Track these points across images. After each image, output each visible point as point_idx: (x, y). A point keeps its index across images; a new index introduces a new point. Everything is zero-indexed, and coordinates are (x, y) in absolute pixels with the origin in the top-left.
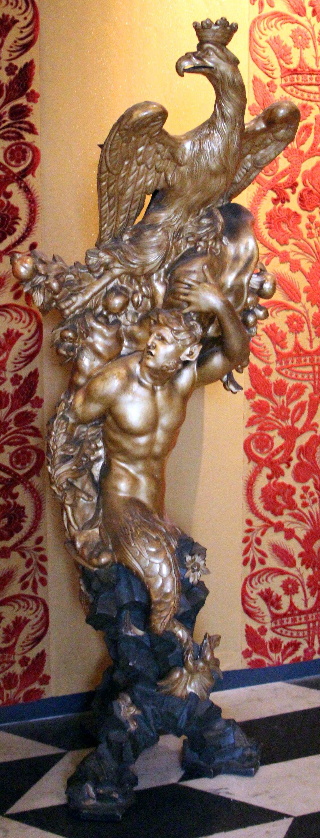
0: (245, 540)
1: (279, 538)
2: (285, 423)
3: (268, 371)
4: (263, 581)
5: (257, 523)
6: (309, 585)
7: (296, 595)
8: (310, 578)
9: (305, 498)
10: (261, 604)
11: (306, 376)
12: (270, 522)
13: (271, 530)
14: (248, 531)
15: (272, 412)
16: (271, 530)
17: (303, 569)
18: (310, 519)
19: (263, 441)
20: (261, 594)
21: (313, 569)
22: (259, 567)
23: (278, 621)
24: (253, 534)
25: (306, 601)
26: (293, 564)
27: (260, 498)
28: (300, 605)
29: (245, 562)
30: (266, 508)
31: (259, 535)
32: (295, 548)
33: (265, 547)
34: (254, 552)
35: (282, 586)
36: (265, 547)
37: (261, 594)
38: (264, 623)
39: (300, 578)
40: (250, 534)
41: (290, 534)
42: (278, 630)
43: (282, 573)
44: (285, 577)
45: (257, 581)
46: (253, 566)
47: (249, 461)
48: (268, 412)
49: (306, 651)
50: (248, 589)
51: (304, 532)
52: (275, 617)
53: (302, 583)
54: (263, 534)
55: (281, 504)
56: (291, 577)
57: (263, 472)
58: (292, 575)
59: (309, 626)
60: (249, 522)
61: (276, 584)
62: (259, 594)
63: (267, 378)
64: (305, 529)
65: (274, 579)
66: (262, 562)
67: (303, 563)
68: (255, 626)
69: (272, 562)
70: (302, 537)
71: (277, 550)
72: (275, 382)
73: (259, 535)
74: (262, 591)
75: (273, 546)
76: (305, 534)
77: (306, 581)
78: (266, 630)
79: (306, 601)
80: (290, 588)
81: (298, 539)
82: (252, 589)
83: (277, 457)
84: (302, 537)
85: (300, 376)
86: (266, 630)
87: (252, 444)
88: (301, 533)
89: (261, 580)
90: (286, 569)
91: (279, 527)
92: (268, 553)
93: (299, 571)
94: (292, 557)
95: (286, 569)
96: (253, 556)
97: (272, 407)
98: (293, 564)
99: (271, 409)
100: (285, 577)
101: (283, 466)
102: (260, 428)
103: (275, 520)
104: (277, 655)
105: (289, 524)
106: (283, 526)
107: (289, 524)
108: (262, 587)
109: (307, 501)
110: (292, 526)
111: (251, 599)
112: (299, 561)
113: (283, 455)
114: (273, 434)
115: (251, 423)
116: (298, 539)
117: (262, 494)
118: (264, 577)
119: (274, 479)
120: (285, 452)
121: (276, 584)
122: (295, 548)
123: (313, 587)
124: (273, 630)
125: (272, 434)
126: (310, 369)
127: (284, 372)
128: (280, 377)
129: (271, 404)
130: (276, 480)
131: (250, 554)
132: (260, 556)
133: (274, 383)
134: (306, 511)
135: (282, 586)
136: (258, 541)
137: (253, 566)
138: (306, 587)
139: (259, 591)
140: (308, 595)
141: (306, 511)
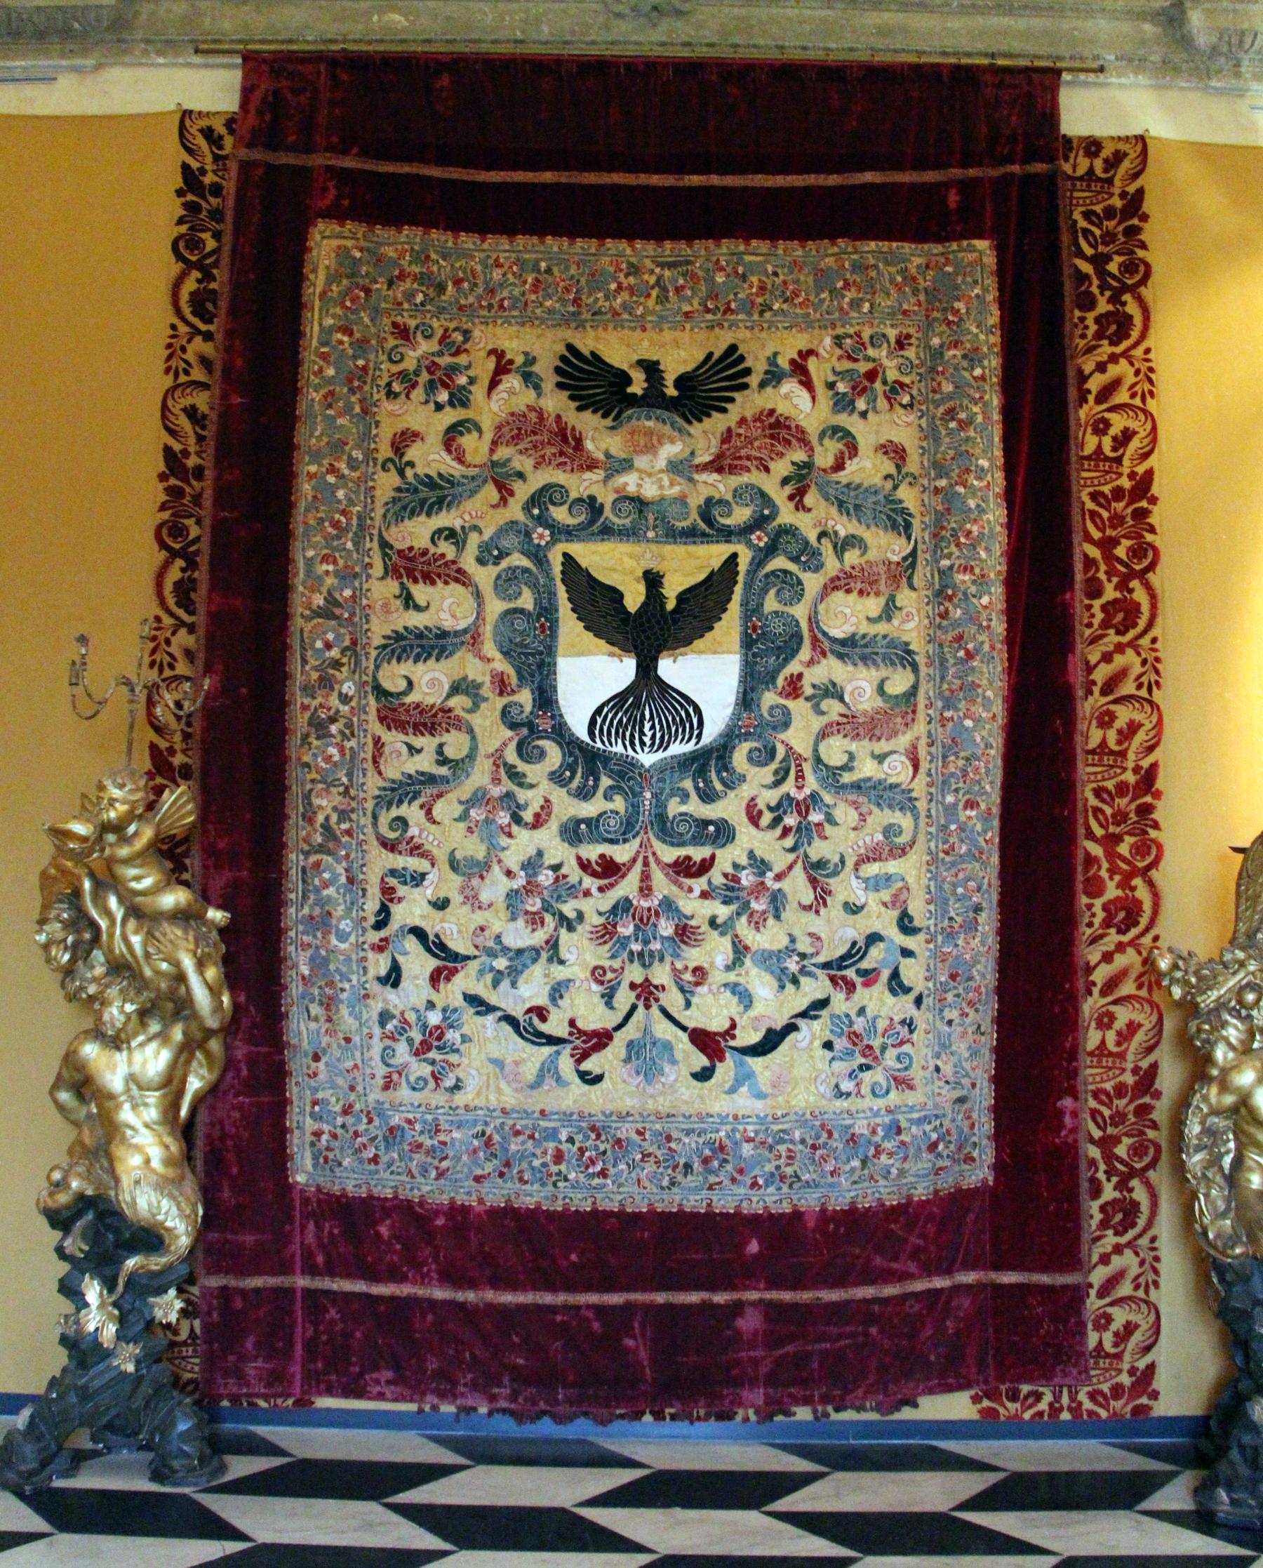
0: (169, 346)
14: (172, 337)
20: (184, 410)
22: (183, 378)
29: (167, 371)
36: (189, 356)
37: (184, 410)
46: (176, 376)
50: (170, 403)
60: (173, 327)
66: (187, 373)
68: (177, 447)
83: (208, 261)
87: (181, 244)
102: (190, 229)
108: (187, 401)
128: (216, 179)
131: (173, 363)
137: (176, 376)
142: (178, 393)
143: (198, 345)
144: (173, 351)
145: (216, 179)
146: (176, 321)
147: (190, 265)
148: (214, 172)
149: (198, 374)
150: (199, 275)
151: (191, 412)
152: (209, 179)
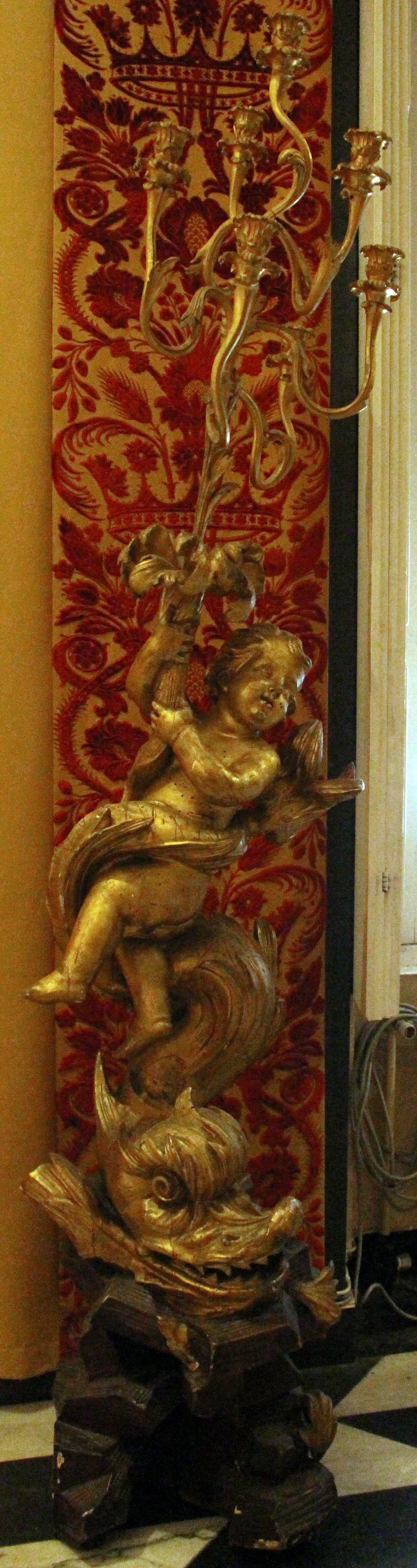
1: (119, 366)
2: (129, 171)
3: (97, 81)
4: (92, 441)
5: (81, 336)
7: (152, 473)
8: (177, 445)
9: (167, 304)
10: (89, 482)
11: (164, 98)
12: (103, 336)
13: (105, 351)
15: (103, 150)
16: (105, 351)
17: (164, 428)
18: (174, 337)
19: (91, 200)
20: (88, 465)
21: (185, 432)
22: (84, 415)
24: (72, 356)
26: (145, 417)
27: (85, 293)
28: (160, 492)
30: (97, 310)
31: (83, 356)
32: (151, 389)
33: (93, 379)
34: (73, 386)
35: (126, 454)
36: (93, 379)
37: (88, 465)
38: (98, 520)
39: (160, 444)
40: (66, 354)
41: (140, 364)
43: (129, 430)
44: (132, 438)
45: (81, 440)
47: (63, 230)
48: (98, 151)
50: (66, 454)
51: (167, 363)
53: (164, 454)
54: (90, 356)
55: (122, 309)
56: (143, 440)
57: (89, 248)
58: (146, 436)
60: (65, 333)
61: (115, 449)
62: (84, 464)
63: (94, 92)
64: (167, 358)
65: (110, 439)
66: (90, 406)
67: (164, 418)
68: (81, 523)
69: (106, 408)
70: (162, 372)
71: (118, 388)
72: (109, 100)
73: (83, 356)
74: (90, 459)
75: (108, 381)
76: (168, 366)
77: (170, 452)
79: (171, 488)
80: (143, 457)
81: (154, 373)
82: (72, 454)
83: (114, 227)
84: (162, 372)
85: (154, 97)
86: (101, 533)
87: (70, 200)
88: (160, 364)
89: (88, 438)
90: (134, 424)
91: (119, 347)
92: (100, 390)
93: (156, 430)
94: (143, 404)
95: (134, 424)
96: (73, 394)
97: (105, 142)
98: (145, 417)
99: (102, 144)
100: (132, 438)
101: (126, 244)
102: (83, 174)
103: (113, 334)
105: (138, 345)
106: (128, 347)
107: (138, 345)
108: (91, 452)
109: (171, 309)
110: (144, 349)
111: (71, 471)
112: (156, 413)
113: (125, 225)
114: (108, 186)
115: (66, 163)
116: (154, 373)
117: (89, 287)
118: (93, 434)
119: (111, 263)
120: (129, 221)
121: (115, 449)
122: (151, 389)
125: (103, 186)
126: (172, 87)
127: (124, 85)
128: (118, 94)
129: (102, 136)
130: (114, 267)
132: (85, 394)
133: (107, 103)
134: (168, 325)
135: (126, 454)
136: (83, 369)
139: (84, 459)
140: (175, 476)
141: (168, 325)
142: (78, 438)
143: (107, 362)
144: (65, 369)
145: (118, 94)
146: (70, 324)
147: (86, 235)
148: (115, 82)
149: (106, 408)
150: (102, 251)
151: (101, 467)
152: (108, 93)
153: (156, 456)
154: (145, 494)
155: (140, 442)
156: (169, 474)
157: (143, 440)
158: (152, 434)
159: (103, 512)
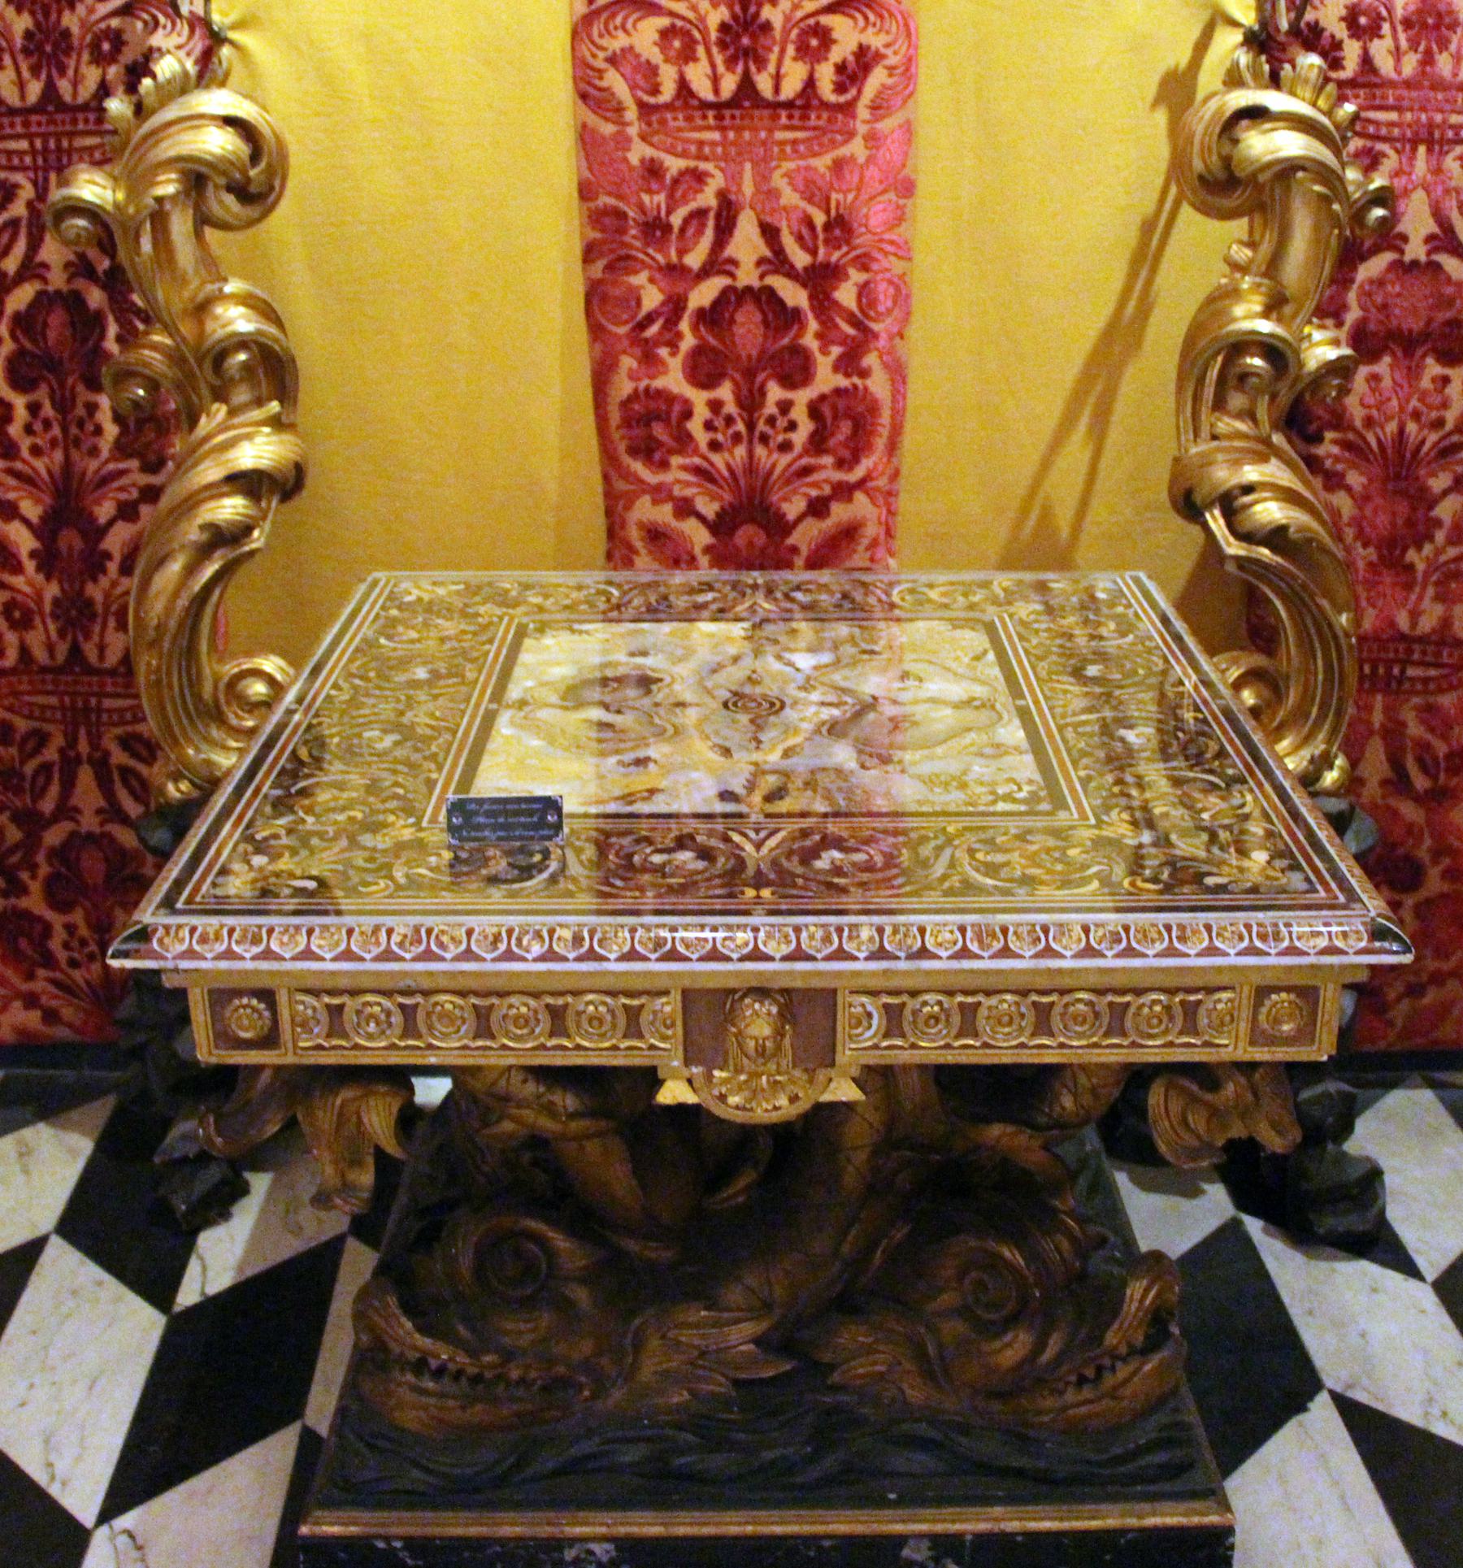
6: (722, 45)
23: (654, 118)
25: (715, 80)
28: (702, 87)
42: (655, 139)
49: (722, 195)
52: (645, 109)
56: (679, 23)
58: (683, 18)
59: (725, 137)
77: (714, 35)
78: (629, 140)
104: (656, 198)
118: (619, 20)
123: (732, 50)
124: (643, 138)
138: (715, 50)
153: (695, 42)
154: (683, 86)
155: (673, 26)
156: (713, 66)
157: (679, 23)
158: (691, 15)
159: (632, 114)
